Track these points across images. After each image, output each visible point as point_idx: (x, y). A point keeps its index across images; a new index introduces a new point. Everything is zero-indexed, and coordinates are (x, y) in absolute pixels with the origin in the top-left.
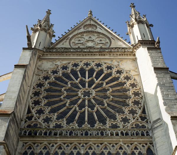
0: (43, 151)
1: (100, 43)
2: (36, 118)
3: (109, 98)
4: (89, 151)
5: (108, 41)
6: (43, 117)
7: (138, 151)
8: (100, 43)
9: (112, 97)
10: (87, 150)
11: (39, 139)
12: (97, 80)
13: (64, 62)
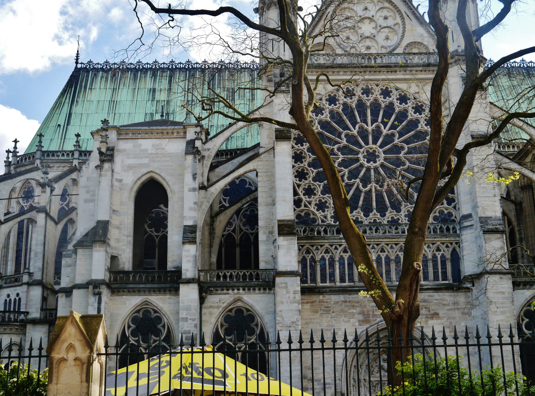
0: (325, 255)
1: (385, 27)
3: (404, 164)
4: (381, 254)
5: (399, 20)
6: (315, 200)
7: (441, 253)
8: (385, 27)
9: (408, 164)
10: (379, 253)
11: (319, 241)
12: (385, 129)
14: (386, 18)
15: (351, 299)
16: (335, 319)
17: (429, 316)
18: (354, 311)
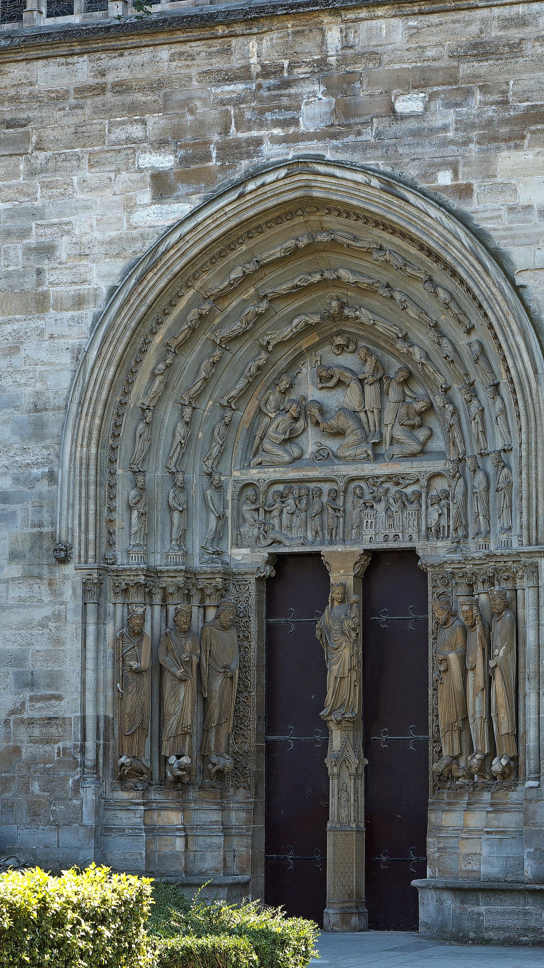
15: (125, 74)
16: (49, 178)
17: (504, 130)
18: (137, 131)
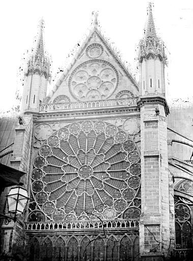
2: (39, 206)
13: (64, 125)
14: (107, 76)
